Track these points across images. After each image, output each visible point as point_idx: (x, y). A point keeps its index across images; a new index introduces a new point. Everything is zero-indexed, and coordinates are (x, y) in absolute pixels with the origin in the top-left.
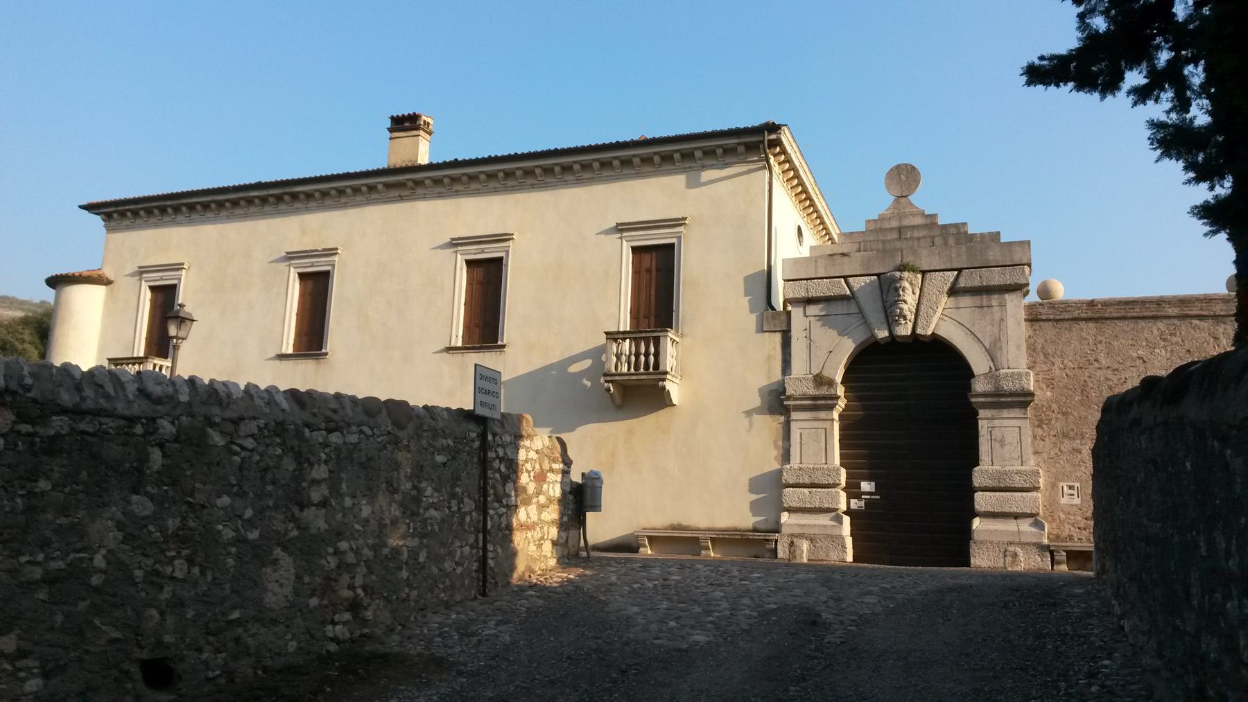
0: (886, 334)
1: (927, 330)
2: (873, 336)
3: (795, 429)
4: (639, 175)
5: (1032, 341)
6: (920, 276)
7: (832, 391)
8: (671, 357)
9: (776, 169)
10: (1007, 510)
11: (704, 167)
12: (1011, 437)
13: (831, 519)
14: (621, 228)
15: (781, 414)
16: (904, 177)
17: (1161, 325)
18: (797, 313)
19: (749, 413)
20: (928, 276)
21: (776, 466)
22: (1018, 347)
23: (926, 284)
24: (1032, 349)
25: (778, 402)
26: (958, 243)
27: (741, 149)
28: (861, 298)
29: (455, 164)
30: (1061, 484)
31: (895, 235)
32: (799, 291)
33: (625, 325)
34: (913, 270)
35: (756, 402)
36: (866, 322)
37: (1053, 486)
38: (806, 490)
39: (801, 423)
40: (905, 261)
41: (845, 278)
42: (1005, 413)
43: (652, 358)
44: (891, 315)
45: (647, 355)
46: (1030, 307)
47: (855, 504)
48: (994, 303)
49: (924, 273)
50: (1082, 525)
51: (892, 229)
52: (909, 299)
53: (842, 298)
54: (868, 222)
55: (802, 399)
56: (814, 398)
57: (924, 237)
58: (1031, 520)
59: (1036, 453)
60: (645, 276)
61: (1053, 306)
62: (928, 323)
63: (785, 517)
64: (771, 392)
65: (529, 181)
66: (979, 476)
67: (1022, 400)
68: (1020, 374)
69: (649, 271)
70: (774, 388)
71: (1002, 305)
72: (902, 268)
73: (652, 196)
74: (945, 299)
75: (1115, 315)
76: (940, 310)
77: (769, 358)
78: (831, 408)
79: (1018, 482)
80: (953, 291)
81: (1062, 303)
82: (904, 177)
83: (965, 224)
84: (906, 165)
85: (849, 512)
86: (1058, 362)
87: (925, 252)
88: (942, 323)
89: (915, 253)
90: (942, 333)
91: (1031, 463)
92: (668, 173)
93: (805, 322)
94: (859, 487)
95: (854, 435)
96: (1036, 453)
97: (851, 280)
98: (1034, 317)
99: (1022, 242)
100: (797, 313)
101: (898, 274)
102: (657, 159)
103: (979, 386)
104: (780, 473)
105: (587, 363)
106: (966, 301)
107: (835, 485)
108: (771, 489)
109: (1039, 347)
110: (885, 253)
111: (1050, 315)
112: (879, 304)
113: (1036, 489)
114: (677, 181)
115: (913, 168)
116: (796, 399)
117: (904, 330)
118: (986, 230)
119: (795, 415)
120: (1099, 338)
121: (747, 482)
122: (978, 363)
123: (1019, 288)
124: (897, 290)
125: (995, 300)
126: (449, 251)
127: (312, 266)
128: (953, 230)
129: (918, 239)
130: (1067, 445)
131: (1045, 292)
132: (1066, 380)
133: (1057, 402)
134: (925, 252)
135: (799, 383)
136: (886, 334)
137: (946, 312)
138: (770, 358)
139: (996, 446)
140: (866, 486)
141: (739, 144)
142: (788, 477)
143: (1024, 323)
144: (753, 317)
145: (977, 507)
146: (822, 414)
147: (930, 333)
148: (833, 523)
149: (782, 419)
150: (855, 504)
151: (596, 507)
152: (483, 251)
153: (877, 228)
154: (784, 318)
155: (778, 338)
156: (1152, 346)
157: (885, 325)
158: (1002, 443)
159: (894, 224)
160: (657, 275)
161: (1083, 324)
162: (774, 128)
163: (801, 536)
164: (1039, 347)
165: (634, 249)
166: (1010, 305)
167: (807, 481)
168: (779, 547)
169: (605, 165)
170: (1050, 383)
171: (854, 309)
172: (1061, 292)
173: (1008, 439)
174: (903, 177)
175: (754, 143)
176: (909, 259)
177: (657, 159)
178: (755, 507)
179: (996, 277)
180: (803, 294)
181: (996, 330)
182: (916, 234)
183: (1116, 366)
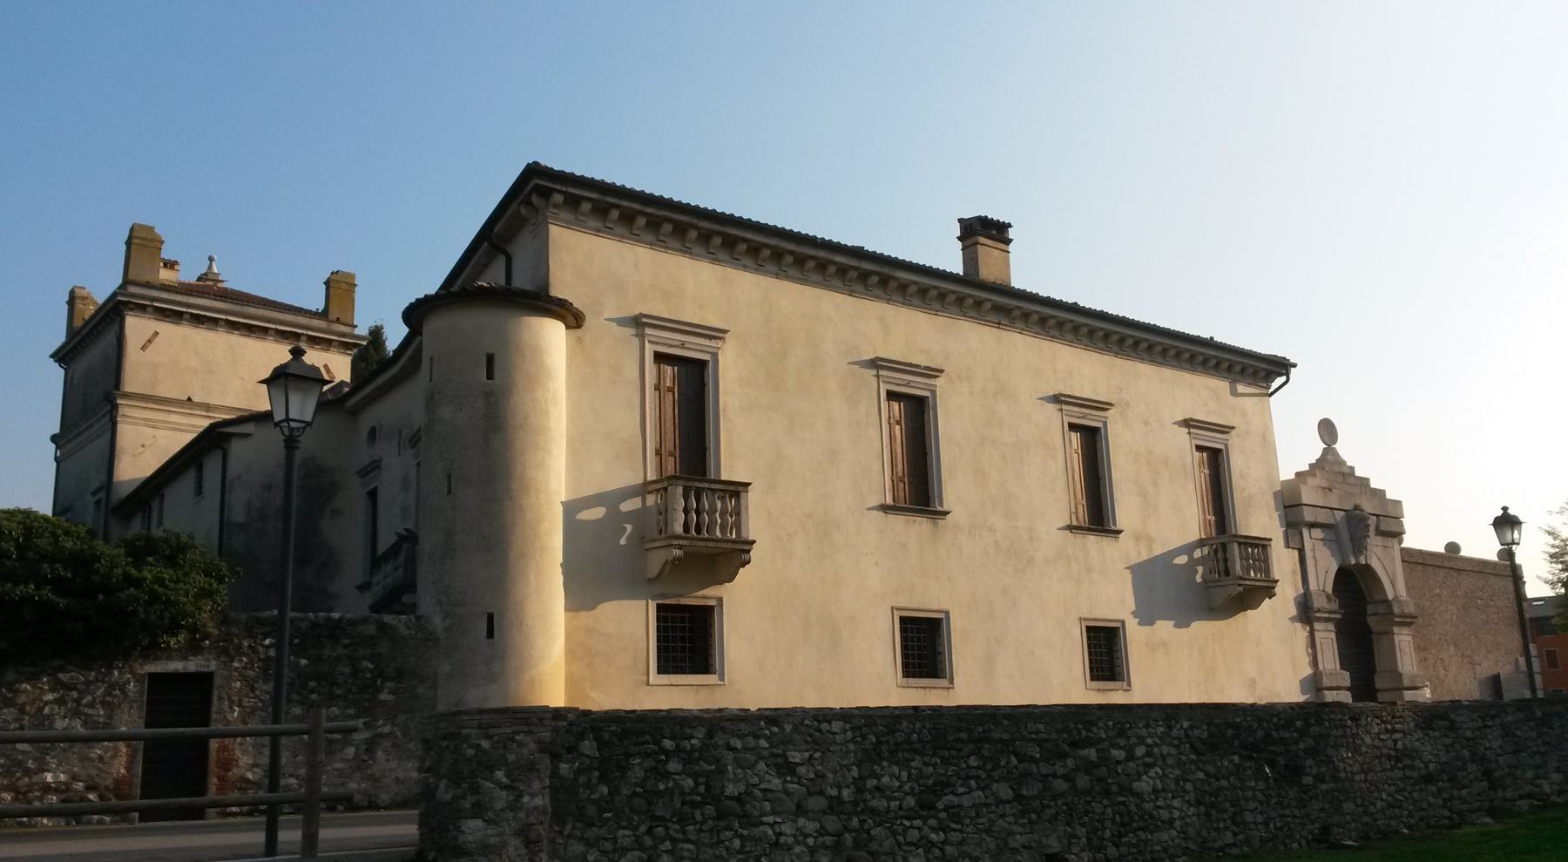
3: (1318, 635)
16: (1327, 430)
35: (1293, 611)
44: (1359, 547)
77: (1294, 572)
82: (1327, 430)
100: (1305, 532)
114: (1221, 385)
126: (1052, 408)
127: (908, 385)
152: (1085, 417)
155: (1296, 553)
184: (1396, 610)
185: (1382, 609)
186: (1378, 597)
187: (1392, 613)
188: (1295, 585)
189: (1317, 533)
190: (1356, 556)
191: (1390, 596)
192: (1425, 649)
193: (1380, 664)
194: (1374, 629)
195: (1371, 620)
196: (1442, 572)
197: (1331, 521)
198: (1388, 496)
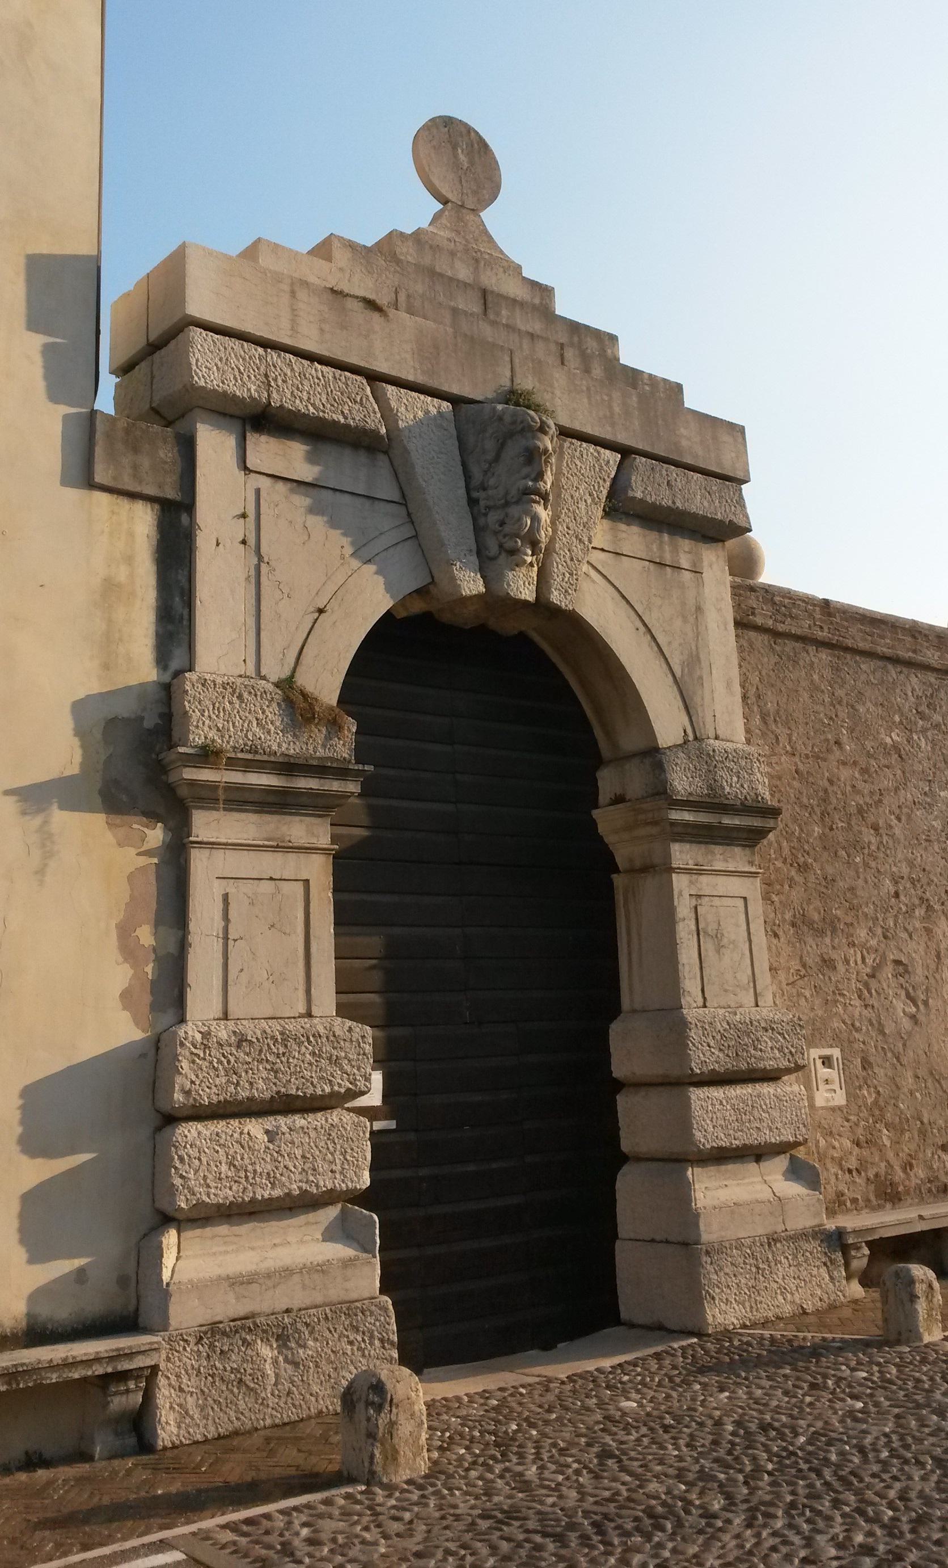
3: (205, 872)
13: (328, 1236)
15: (152, 816)
21: (125, 1030)
25: (145, 764)
35: (62, 754)
38: (255, 1128)
48: (685, 563)
50: (853, 1163)
56: (288, 767)
58: (781, 1162)
64: (112, 724)
70: (125, 709)
119: (206, 824)
138: (110, 591)
149: (156, 835)
156: (908, 728)
163: (245, 1327)
167: (263, 1089)
168: (164, 1395)
171: (387, 490)
184: (682, 781)
185: (635, 780)
186: (630, 742)
187: (661, 792)
188: (108, 645)
189: (293, 458)
190: (486, 564)
191: (667, 725)
192: (830, 926)
193: (634, 988)
194: (622, 856)
195: (607, 821)
196: (915, 681)
197: (353, 406)
198: (691, 401)
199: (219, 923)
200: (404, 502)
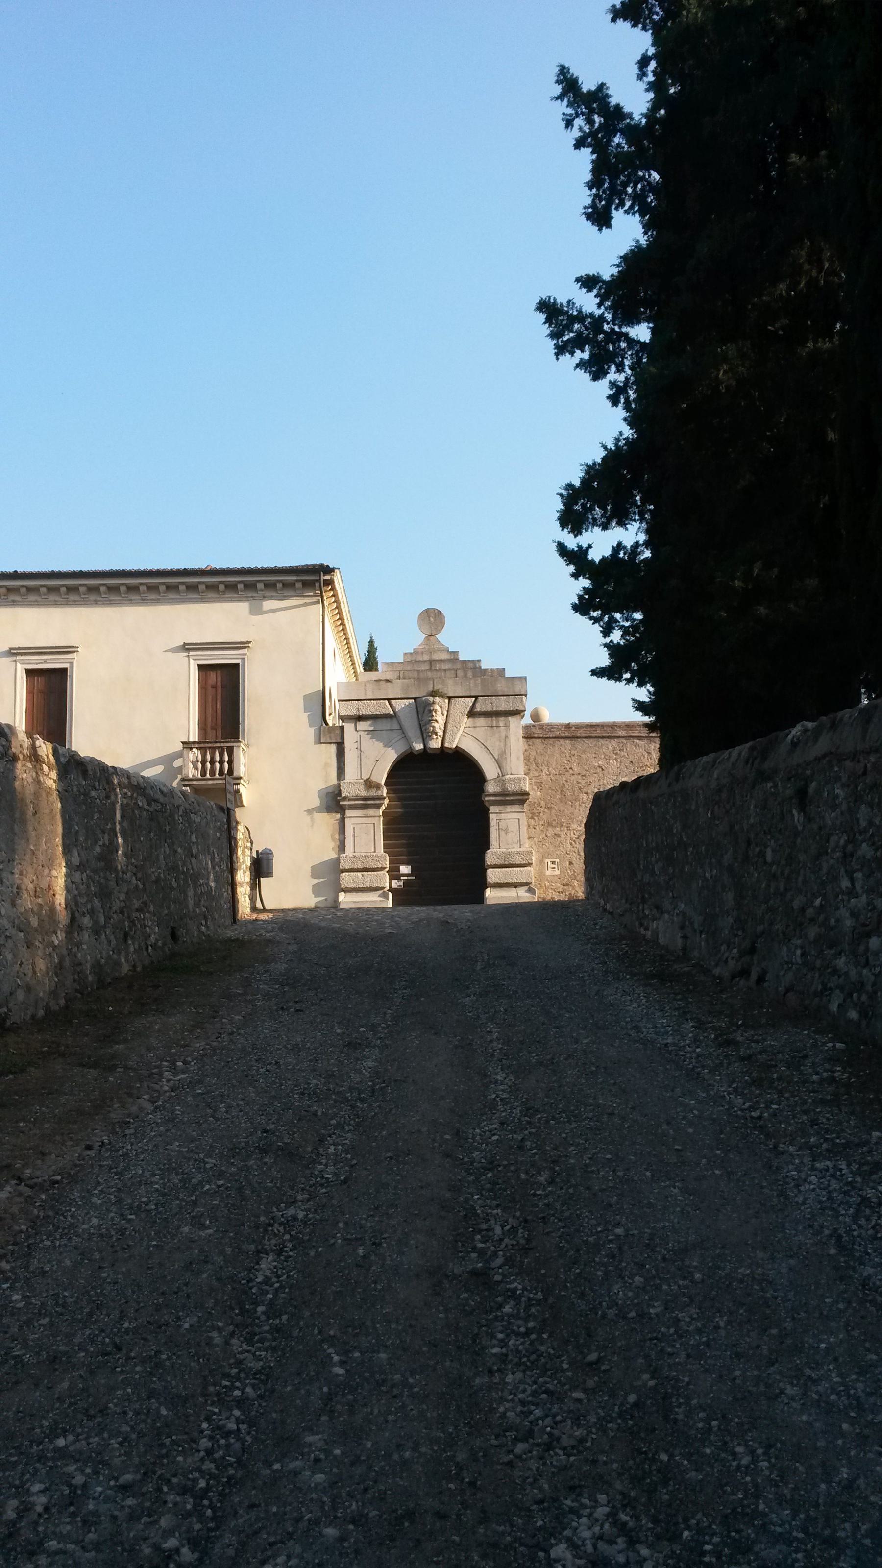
0: (422, 747)
1: (451, 744)
2: (411, 748)
4: (203, 600)
5: (527, 753)
6: (447, 701)
7: (379, 793)
8: (243, 763)
9: (326, 603)
10: (510, 881)
11: (264, 598)
12: (513, 826)
14: (187, 648)
15: (337, 812)
16: (433, 619)
17: (614, 743)
18: (349, 727)
19: (310, 812)
20: (453, 700)
21: (333, 855)
22: (518, 758)
23: (452, 707)
24: (527, 759)
25: (335, 802)
26: (474, 676)
27: (299, 585)
28: (401, 716)
29: (15, 575)
30: (547, 860)
31: (426, 667)
32: (351, 710)
33: (194, 737)
34: (442, 696)
35: (316, 802)
36: (405, 737)
37: (541, 862)
38: (359, 874)
39: (354, 819)
40: (436, 688)
41: (389, 700)
42: (509, 808)
43: (226, 766)
44: (425, 733)
45: (221, 762)
46: (527, 728)
47: (395, 884)
48: (501, 724)
49: (450, 698)
50: (560, 890)
51: (425, 661)
52: (440, 718)
53: (387, 717)
54: (405, 654)
55: (355, 800)
56: (365, 799)
57: (449, 670)
58: (526, 888)
59: (529, 838)
60: (210, 691)
61: (542, 727)
62: (454, 738)
63: (342, 896)
64: (328, 794)
65: (92, 597)
66: (490, 857)
67: (521, 798)
68: (519, 779)
69: (214, 687)
71: (507, 726)
72: (434, 694)
73: (218, 621)
74: (466, 719)
75: (584, 735)
76: (462, 729)
77: (326, 765)
78: (378, 806)
79: (518, 860)
80: (472, 714)
81: (548, 725)
82: (433, 619)
83: (479, 661)
84: (434, 609)
85: (391, 890)
86: (545, 770)
87: (450, 682)
88: (463, 738)
89: (443, 682)
90: (463, 746)
91: (527, 846)
92: (231, 600)
93: (356, 736)
94: (399, 871)
95: (397, 831)
96: (529, 838)
97: (393, 701)
98: (529, 736)
99: (520, 678)
101: (431, 699)
102: (222, 587)
103: (491, 788)
104: (337, 860)
105: (159, 769)
106: (481, 721)
107: (383, 869)
108: (331, 874)
109: (532, 758)
110: (420, 680)
111: (540, 734)
112: (416, 723)
113: (530, 864)
114: (241, 608)
115: (440, 612)
116: (350, 800)
117: (435, 744)
118: (495, 667)
119: (349, 813)
120: (573, 752)
121: (309, 869)
122: (490, 770)
123: (518, 713)
124: (430, 711)
125: (502, 721)
128: (471, 665)
129: (445, 670)
130: (550, 832)
131: (536, 717)
132: (550, 784)
133: (544, 800)
134: (450, 682)
135: (352, 787)
136: (422, 747)
137: (467, 730)
139: (502, 833)
140: (405, 869)
141: (297, 581)
142: (344, 864)
143: (521, 740)
144: (312, 731)
145: (489, 880)
146: (371, 812)
147: (454, 746)
148: (381, 899)
149: (338, 816)
150: (395, 884)
151: (269, 874)
152: (45, 662)
153: (412, 660)
154: (338, 731)
155: (333, 748)
156: (608, 758)
157: (421, 740)
158: (506, 831)
159: (426, 657)
160: (223, 693)
161: (562, 741)
162: (329, 570)
164: (532, 758)
165: (201, 667)
166: (512, 726)
167: (360, 866)
169: (170, 588)
170: (540, 786)
172: (547, 717)
173: (511, 828)
174: (432, 619)
175: (312, 580)
176: (438, 687)
177: (222, 587)
178: (316, 890)
179: (503, 704)
180: (354, 712)
181: (502, 745)
182: (444, 666)
183: (584, 773)
198: (508, 674)
199: (352, 833)
200: (401, 728)
